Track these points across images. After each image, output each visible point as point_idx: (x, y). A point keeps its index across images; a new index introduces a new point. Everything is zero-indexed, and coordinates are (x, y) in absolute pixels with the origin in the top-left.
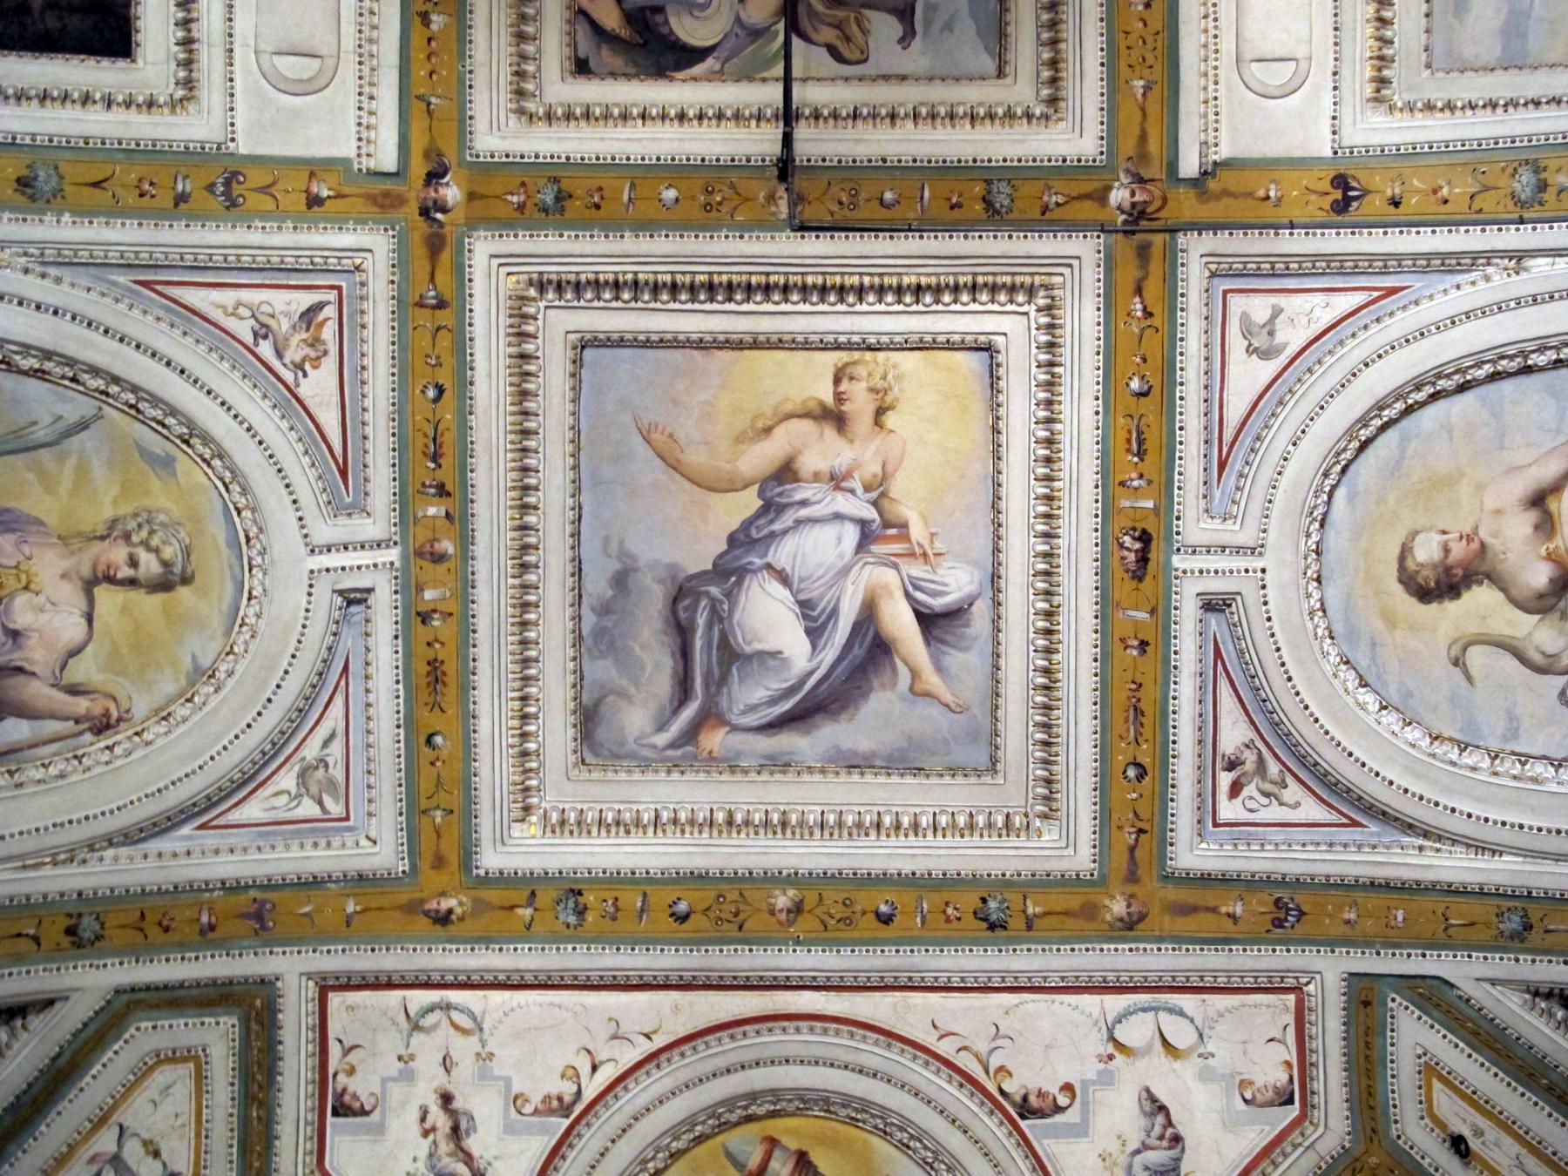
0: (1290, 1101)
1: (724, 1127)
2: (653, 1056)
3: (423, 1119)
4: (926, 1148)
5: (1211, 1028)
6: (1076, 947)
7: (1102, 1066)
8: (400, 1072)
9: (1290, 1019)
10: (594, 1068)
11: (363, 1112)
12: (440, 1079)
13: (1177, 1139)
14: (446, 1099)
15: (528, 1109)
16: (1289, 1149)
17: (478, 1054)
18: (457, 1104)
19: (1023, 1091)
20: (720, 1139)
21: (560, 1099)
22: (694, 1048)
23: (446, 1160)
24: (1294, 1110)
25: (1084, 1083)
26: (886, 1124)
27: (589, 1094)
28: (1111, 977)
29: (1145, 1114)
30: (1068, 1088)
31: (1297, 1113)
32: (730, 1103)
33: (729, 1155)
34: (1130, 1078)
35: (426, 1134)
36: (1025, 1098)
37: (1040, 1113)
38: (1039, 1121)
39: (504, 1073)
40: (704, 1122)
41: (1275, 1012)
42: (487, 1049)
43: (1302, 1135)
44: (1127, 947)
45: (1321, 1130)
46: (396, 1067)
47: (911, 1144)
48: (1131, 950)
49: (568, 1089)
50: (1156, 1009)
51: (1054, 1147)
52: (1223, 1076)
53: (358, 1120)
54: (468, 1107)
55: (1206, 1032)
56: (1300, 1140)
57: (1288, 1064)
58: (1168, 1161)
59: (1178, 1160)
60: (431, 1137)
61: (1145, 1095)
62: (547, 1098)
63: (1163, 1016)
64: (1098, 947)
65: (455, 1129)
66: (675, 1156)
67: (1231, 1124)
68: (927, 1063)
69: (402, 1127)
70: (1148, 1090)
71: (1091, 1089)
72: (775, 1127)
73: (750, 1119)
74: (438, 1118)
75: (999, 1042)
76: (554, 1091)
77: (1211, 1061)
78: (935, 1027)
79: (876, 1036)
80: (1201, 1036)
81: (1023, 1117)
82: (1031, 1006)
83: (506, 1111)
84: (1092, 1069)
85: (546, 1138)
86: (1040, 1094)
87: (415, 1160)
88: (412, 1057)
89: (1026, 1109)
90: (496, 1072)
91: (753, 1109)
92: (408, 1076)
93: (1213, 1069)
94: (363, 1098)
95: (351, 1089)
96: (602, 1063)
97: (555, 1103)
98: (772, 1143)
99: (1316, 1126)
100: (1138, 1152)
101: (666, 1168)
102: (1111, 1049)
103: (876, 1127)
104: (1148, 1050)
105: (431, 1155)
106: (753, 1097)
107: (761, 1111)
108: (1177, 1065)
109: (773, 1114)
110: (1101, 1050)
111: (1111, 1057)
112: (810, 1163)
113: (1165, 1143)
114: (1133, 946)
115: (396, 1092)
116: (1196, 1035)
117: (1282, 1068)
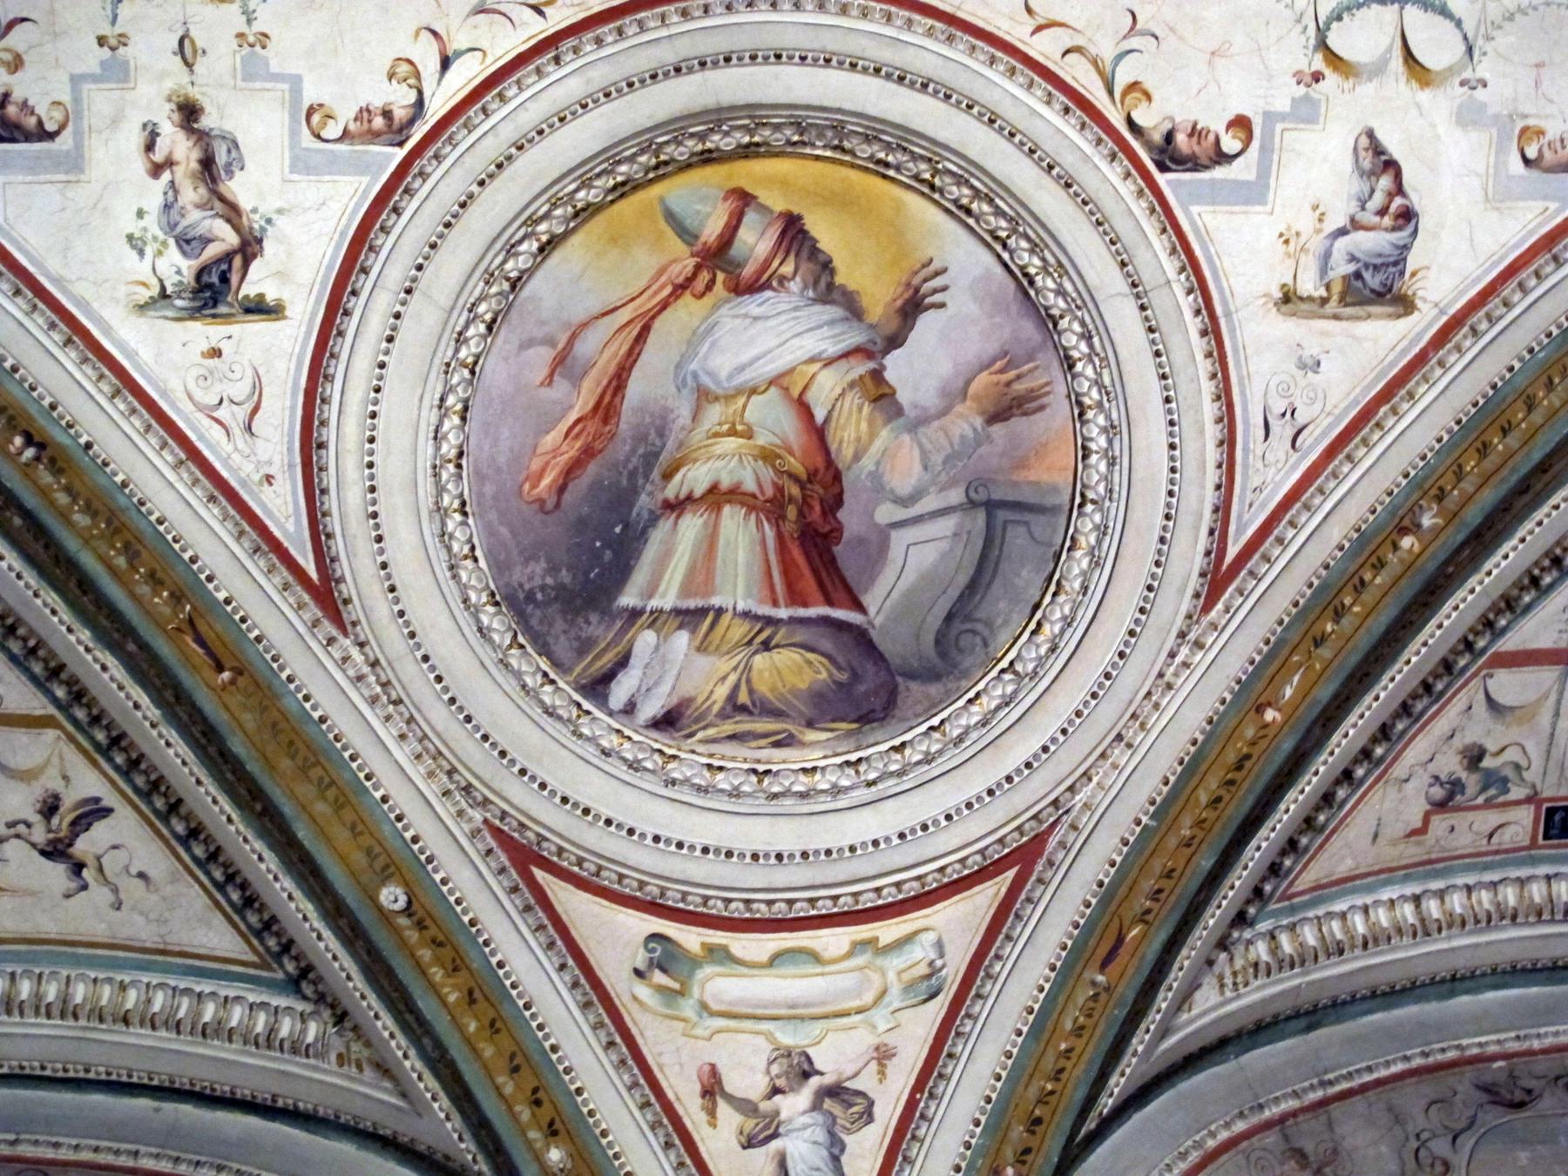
1: (663, 170)
2: (549, 43)
3: (150, 147)
4: (999, 212)
5: (1489, 38)
7: (1302, 90)
8: (103, 64)
10: (445, 63)
11: (42, 134)
12: (176, 78)
13: (1407, 216)
14: (189, 112)
15: (332, 131)
17: (240, 35)
18: (206, 122)
19: (1168, 126)
20: (656, 190)
21: (387, 114)
22: (620, 31)
23: (194, 215)
25: (1270, 117)
26: (935, 172)
27: (437, 108)
29: (1362, 173)
30: (1241, 124)
32: (678, 126)
33: (670, 217)
34: (1348, 110)
35: (156, 170)
36: (1169, 137)
37: (1191, 163)
38: (1187, 176)
39: (292, 68)
40: (631, 159)
42: (258, 26)
46: (94, 57)
47: (974, 206)
49: (401, 98)
51: (1207, 218)
52: (1497, 117)
53: (37, 146)
54: (228, 126)
58: (1388, 250)
59: (1406, 248)
60: (166, 176)
61: (1364, 141)
62: (365, 113)
65: (207, 163)
66: (584, 214)
67: (1498, 196)
68: (1013, 71)
69: (114, 156)
70: (1370, 134)
71: (1279, 127)
72: (747, 173)
73: (708, 158)
74: (175, 142)
75: (1134, 42)
76: (377, 103)
77: (1480, 93)
78: (1029, 10)
80: (1470, 50)
81: (1163, 168)
83: (294, 134)
85: (365, 180)
86: (1195, 132)
87: (140, 214)
88: (123, 40)
89: (1169, 155)
90: (274, 67)
91: (715, 141)
92: (117, 72)
93: (1483, 106)
94: (41, 110)
95: (18, 95)
96: (459, 54)
97: (379, 122)
98: (743, 199)
100: (1342, 232)
101: (567, 234)
102: (1318, 63)
103: (916, 177)
104: (1378, 70)
105: (167, 207)
106: (718, 117)
107: (727, 143)
108: (1425, 96)
109: (748, 152)
110: (1303, 64)
111: (1317, 77)
112: (803, 233)
113: (1387, 221)
115: (99, 101)
116: (1463, 48)
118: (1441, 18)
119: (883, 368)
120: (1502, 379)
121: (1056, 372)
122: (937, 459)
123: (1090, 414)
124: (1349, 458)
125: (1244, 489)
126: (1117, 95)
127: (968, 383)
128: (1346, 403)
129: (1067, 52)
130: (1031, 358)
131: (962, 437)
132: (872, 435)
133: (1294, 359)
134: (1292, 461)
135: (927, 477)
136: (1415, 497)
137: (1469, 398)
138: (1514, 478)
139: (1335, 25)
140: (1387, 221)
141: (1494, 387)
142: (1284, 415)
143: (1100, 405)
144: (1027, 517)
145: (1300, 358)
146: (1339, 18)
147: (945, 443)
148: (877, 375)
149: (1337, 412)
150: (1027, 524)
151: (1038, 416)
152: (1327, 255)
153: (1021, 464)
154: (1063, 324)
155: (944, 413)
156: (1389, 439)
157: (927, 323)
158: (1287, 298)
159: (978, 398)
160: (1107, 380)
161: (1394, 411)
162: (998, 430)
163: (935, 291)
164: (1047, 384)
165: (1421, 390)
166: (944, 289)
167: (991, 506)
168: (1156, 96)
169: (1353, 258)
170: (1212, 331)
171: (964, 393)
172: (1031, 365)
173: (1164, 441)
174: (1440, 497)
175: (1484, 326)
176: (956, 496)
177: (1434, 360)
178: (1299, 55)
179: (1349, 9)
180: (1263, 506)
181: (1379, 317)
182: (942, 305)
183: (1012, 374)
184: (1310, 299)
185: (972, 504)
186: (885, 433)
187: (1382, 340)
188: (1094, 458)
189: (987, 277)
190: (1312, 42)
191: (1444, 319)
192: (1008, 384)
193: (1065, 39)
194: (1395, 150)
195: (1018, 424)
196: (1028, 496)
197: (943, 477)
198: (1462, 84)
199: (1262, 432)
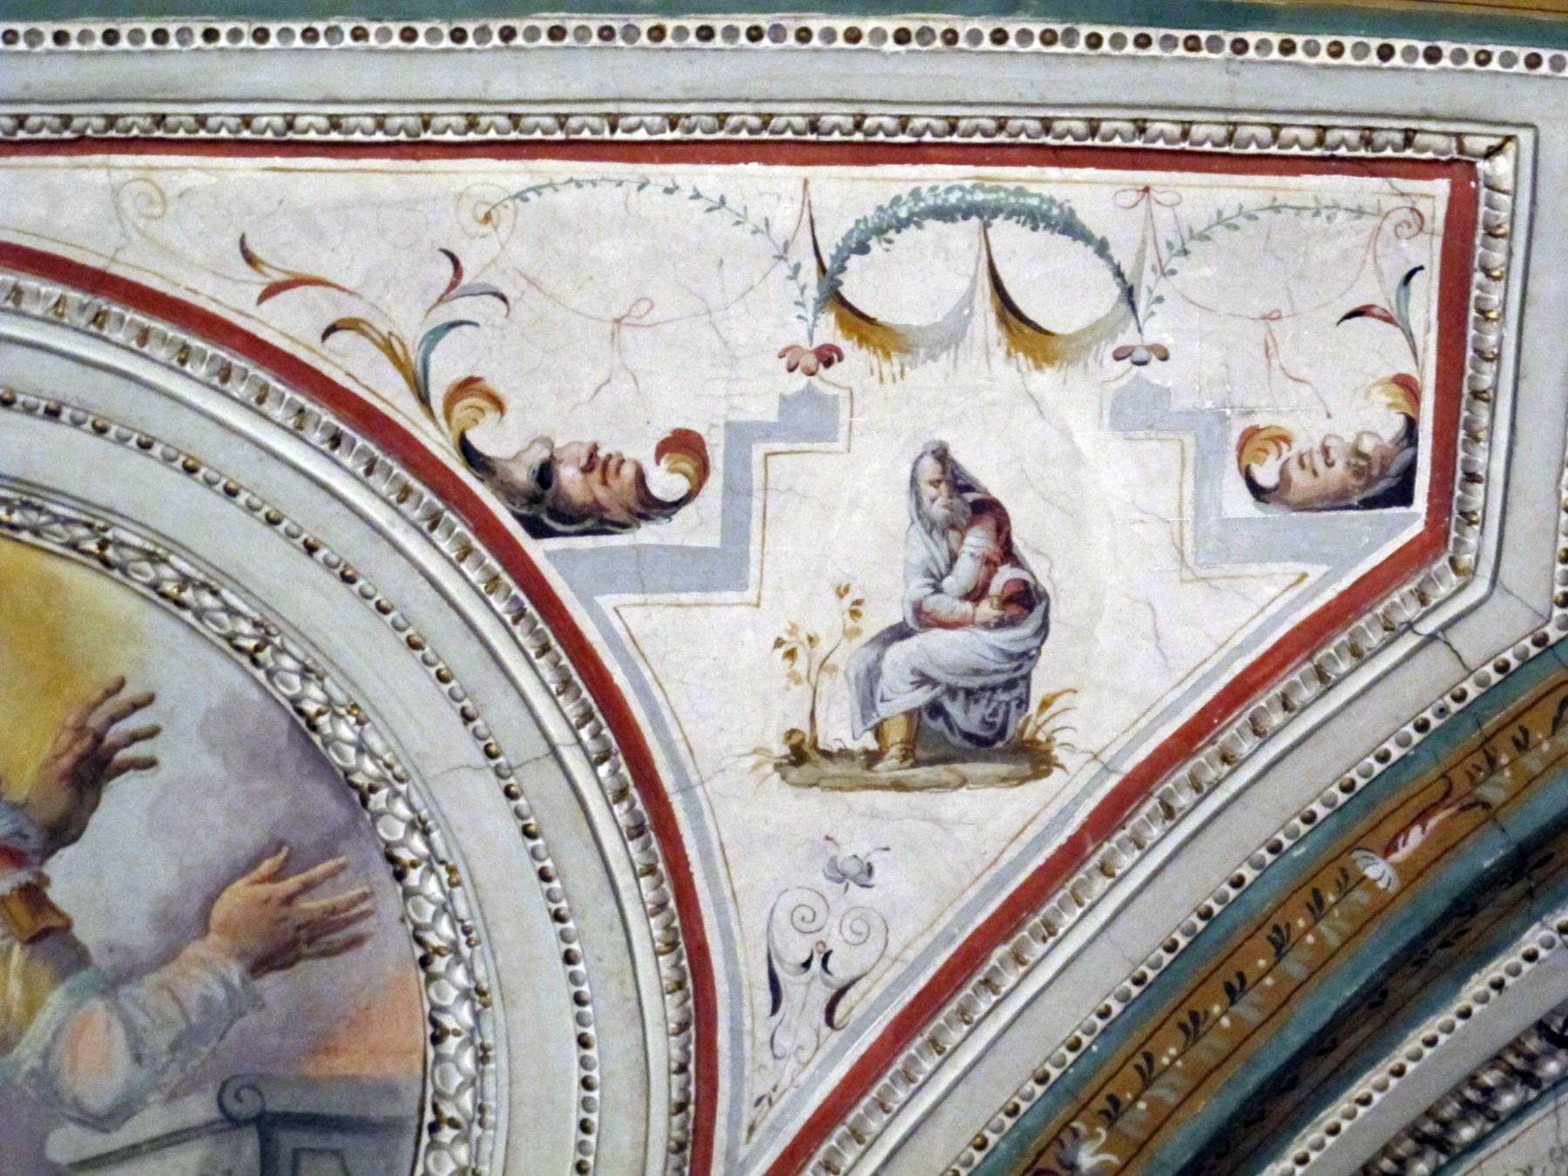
0: (1401, 494)
6: (719, 23)
7: (799, 381)
9: (1428, 252)
13: (1026, 600)
16: (1375, 638)
19: (540, 454)
24: (1412, 521)
25: (739, 434)
28: (836, 117)
29: (931, 526)
30: (684, 445)
31: (1418, 528)
34: (886, 423)
36: (545, 473)
37: (593, 520)
38: (587, 542)
41: (1377, 233)
43: (1423, 599)
44: (890, 25)
45: (1479, 588)
47: (188, 595)
48: (902, 37)
50: (985, 213)
51: (634, 617)
52: (1192, 415)
55: (1147, 282)
56: (1412, 611)
57: (1407, 386)
58: (992, 661)
59: (1027, 657)
61: (930, 468)
63: (1005, 232)
64: (791, 24)
67: (1201, 556)
70: (942, 455)
75: (461, 308)
77: (1155, 372)
78: (250, 259)
79: (54, 290)
80: (1129, 294)
81: (538, 530)
82: (568, 199)
84: (763, 392)
86: (593, 463)
89: (546, 506)
99: (1467, 575)
100: (900, 633)
102: (828, 330)
104: (949, 337)
108: (1044, 380)
110: (797, 334)
111: (828, 356)
114: (913, 24)
117: (1381, 398)
118: (1066, 239)
119: (44, 881)
120: (1221, 900)
121: (383, 872)
122: (160, 1040)
123: (439, 964)
124: (934, 1044)
125: (736, 1100)
126: (437, 404)
127: (211, 900)
128: (928, 939)
129: (331, 330)
130: (328, 850)
131: (207, 1001)
132: (32, 1006)
133: (822, 862)
134: (826, 1049)
135: (141, 1076)
136: (1063, 1113)
137: (1160, 934)
138: (1253, 1080)
139: (855, 261)
140: (987, 610)
141: (1206, 915)
142: (807, 965)
143: (454, 948)
144: (338, 1141)
145: (833, 860)
146: (863, 249)
147: (172, 1011)
148: (34, 895)
149: (910, 955)
150: (336, 1153)
151: (350, 956)
152: (872, 675)
153: (324, 1046)
154: (378, 800)
155: (169, 955)
156: (1006, 1013)
157: (122, 801)
158: (801, 754)
159: (226, 928)
160: (462, 909)
161: (1018, 959)
162: (272, 985)
163: (135, 738)
164: (364, 897)
165: (1068, 920)
166: (152, 733)
167: (267, 1125)
168: (512, 404)
169: (923, 680)
170: (657, 822)
171: (203, 922)
172: (329, 865)
173: (571, 1029)
174: (1113, 1112)
175: (1183, 800)
176: (199, 1108)
177: (1094, 861)
178: (788, 316)
179: (880, 231)
180: (775, 1129)
181: (987, 782)
182: (149, 764)
183: (291, 884)
184: (845, 754)
185: (231, 1122)
186: (56, 1000)
187: (990, 825)
188: (452, 1043)
189: (231, 709)
190: (812, 293)
191: (1113, 782)
192: (289, 900)
193: (330, 309)
194: (992, 480)
195: (311, 973)
196: (336, 1104)
197: (173, 1076)
198: (1119, 356)
199: (765, 997)
